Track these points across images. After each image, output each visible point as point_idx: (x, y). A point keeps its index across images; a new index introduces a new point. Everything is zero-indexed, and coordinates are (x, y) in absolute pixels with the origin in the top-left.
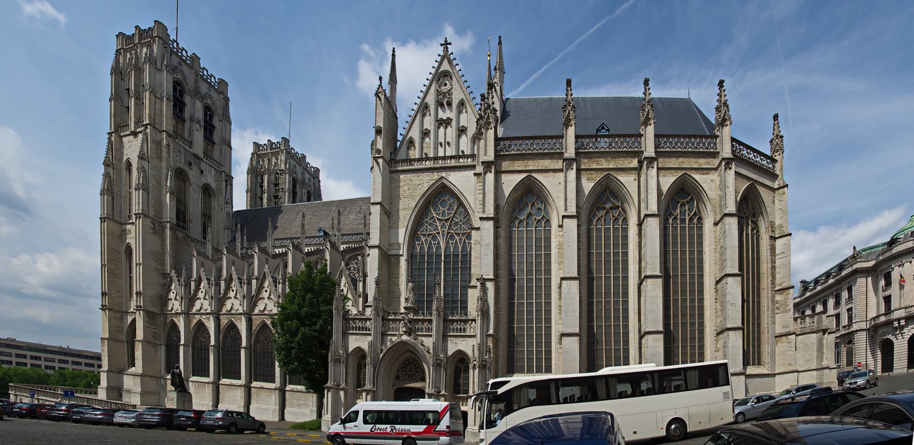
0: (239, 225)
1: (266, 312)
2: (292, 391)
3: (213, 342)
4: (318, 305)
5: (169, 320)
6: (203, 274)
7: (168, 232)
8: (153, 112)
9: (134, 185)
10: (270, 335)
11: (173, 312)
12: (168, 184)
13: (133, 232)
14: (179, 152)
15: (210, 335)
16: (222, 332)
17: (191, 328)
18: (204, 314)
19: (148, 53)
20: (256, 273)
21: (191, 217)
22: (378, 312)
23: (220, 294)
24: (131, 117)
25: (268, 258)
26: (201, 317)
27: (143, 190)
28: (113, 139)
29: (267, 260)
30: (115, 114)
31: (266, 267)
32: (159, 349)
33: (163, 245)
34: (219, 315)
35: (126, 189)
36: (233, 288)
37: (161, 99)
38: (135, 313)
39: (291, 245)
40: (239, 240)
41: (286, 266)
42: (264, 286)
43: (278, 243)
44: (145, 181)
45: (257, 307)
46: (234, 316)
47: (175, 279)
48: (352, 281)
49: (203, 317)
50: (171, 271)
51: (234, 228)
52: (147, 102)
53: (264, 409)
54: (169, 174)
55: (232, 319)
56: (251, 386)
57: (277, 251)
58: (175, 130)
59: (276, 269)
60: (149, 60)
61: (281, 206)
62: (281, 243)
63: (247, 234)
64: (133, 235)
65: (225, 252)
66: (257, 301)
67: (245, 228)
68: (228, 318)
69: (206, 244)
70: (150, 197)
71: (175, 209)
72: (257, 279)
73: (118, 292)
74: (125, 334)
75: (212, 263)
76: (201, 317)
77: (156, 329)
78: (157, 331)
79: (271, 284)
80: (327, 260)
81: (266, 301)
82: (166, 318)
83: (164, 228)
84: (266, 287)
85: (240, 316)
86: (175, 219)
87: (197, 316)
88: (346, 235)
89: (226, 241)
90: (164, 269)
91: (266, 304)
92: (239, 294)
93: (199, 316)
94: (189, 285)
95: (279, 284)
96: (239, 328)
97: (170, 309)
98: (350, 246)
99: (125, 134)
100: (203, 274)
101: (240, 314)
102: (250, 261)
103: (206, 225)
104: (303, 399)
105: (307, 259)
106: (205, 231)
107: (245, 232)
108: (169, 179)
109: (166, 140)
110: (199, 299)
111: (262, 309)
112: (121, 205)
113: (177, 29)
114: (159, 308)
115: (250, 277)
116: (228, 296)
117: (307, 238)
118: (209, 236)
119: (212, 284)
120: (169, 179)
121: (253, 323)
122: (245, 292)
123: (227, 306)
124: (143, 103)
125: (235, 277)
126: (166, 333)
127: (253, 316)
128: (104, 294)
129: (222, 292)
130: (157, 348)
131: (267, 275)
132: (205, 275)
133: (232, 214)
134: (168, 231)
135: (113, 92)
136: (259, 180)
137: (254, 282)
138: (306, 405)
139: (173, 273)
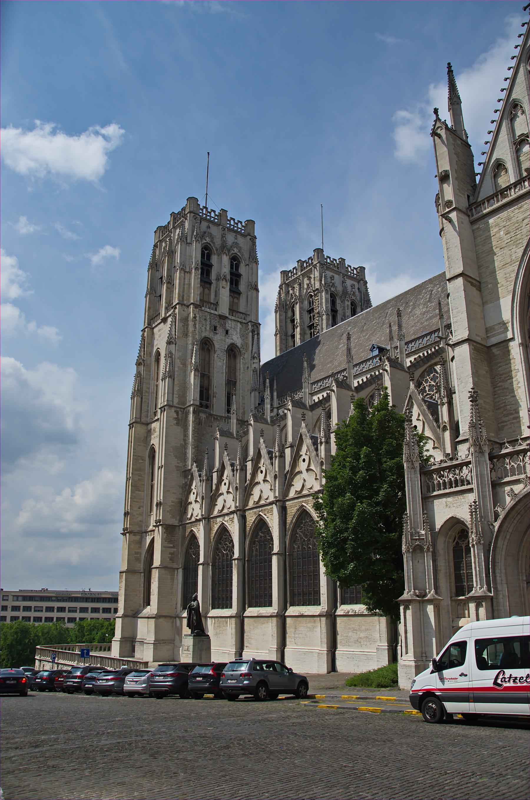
0: (268, 380)
1: (305, 492)
2: (346, 616)
3: (236, 555)
4: (380, 462)
5: (188, 531)
6: (226, 459)
7: (191, 417)
8: (181, 290)
9: (161, 376)
10: (311, 526)
11: (193, 519)
12: (193, 361)
13: (157, 430)
14: (205, 319)
15: (233, 543)
16: (248, 535)
17: (212, 538)
18: (227, 514)
19: (181, 233)
20: (290, 439)
21: (215, 390)
22: (480, 448)
23: (246, 482)
24: (162, 304)
25: (305, 412)
26: (223, 520)
27: (169, 378)
28: (146, 334)
29: (304, 415)
30: (149, 308)
31: (303, 425)
32: (176, 574)
33: (186, 435)
34: (245, 511)
35: (154, 382)
37: (190, 272)
38: (154, 531)
39: (334, 384)
40: (267, 401)
41: (329, 416)
42: (301, 453)
43: (316, 387)
44: (172, 366)
45: (292, 488)
46: (263, 508)
47: (196, 474)
48: (429, 408)
49: (227, 518)
50: (192, 465)
51: (262, 387)
52: (178, 281)
53: (305, 653)
54: (195, 349)
55: (260, 513)
56: (286, 614)
57: (316, 398)
58: (202, 299)
59: (315, 425)
60: (181, 239)
61: (319, 336)
62: (321, 386)
63: (277, 390)
64: (157, 433)
65: (252, 422)
66: (293, 479)
67: (275, 381)
68: (255, 513)
69: (230, 419)
70: (175, 383)
71: (199, 386)
72: (291, 446)
73: (139, 508)
74: (142, 561)
75: (237, 441)
76: (223, 520)
77: (174, 547)
78: (175, 550)
79: (310, 448)
80: (386, 388)
81: (305, 475)
82: (185, 530)
83: (187, 414)
84: (304, 455)
85: (271, 507)
86: (198, 399)
87: (219, 520)
88: (411, 341)
89: (253, 407)
90: (185, 466)
91: (304, 480)
92: (269, 474)
94: (210, 478)
95: (321, 445)
96: (270, 525)
97: (189, 516)
98: (421, 354)
99: (156, 324)
100: (226, 459)
101: (271, 503)
102: (282, 424)
103: (230, 394)
104: (364, 627)
105: (357, 397)
106: (229, 403)
107: (275, 387)
108: (194, 355)
109: (193, 312)
111: (299, 489)
112: (148, 403)
113: (207, 194)
114: (178, 518)
115: (283, 446)
116: (256, 481)
117: (355, 365)
118: (234, 407)
119: (237, 470)
120: (194, 355)
121: (288, 512)
122: (277, 469)
124: (174, 285)
125: (264, 452)
126: (184, 550)
127: (287, 503)
128: (126, 514)
129: (249, 477)
130: (175, 571)
131: (304, 437)
132: (229, 460)
133: (260, 369)
134: (191, 416)
135: (149, 288)
136: (290, 314)
137: (288, 451)
138: (369, 639)
139: (195, 469)
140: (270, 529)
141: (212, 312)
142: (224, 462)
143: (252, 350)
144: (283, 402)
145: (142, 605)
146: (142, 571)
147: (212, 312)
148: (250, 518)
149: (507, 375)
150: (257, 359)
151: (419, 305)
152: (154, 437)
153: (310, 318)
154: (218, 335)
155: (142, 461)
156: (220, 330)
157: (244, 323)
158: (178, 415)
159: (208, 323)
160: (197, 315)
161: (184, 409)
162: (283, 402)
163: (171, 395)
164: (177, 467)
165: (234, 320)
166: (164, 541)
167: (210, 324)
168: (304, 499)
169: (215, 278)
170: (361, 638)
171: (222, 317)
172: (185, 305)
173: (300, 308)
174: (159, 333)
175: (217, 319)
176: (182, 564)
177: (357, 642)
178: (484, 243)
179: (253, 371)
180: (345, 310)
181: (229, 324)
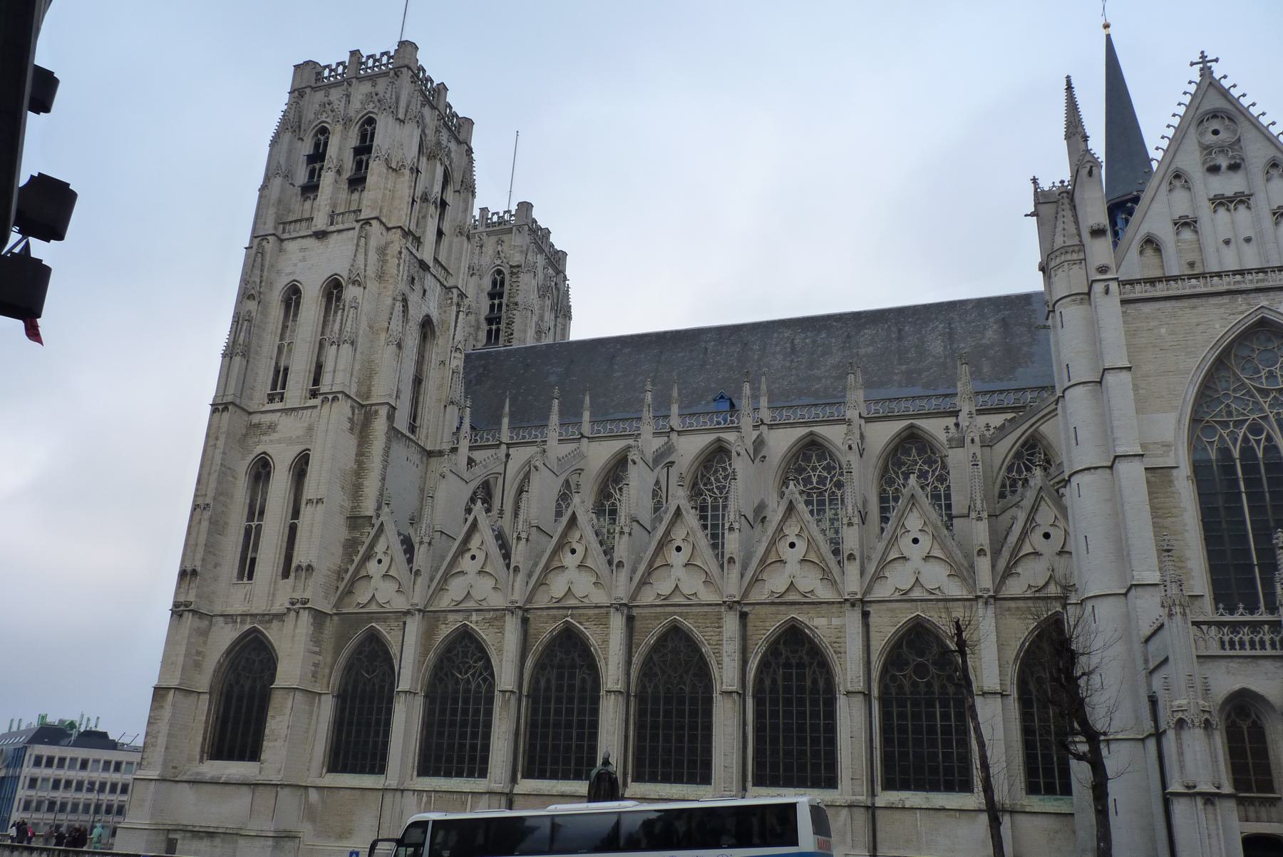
36: (575, 546)
46: (575, 612)
77: (319, 653)
87: (451, 617)
93: (459, 617)
110: (462, 573)
114: (333, 600)
123: (552, 587)
130: (315, 699)
141: (414, 251)
142: (478, 519)
143: (454, 335)
144: (533, 436)
145: (198, 757)
146: (206, 689)
149: (1166, 511)
150: (461, 353)
151: (774, 354)
152: (271, 441)
153: (492, 306)
154: (415, 293)
155: (232, 479)
156: (417, 287)
157: (445, 287)
158: (353, 414)
161: (363, 406)
162: (533, 436)
163: (348, 375)
164: (342, 507)
165: (435, 276)
166: (309, 639)
167: (408, 271)
168: (677, 610)
169: (420, 196)
171: (423, 266)
172: (384, 225)
173: (479, 286)
174: (302, 254)
175: (417, 265)
176: (333, 688)
178: (1134, 335)
179: (453, 372)
180: (543, 310)
181: (429, 282)
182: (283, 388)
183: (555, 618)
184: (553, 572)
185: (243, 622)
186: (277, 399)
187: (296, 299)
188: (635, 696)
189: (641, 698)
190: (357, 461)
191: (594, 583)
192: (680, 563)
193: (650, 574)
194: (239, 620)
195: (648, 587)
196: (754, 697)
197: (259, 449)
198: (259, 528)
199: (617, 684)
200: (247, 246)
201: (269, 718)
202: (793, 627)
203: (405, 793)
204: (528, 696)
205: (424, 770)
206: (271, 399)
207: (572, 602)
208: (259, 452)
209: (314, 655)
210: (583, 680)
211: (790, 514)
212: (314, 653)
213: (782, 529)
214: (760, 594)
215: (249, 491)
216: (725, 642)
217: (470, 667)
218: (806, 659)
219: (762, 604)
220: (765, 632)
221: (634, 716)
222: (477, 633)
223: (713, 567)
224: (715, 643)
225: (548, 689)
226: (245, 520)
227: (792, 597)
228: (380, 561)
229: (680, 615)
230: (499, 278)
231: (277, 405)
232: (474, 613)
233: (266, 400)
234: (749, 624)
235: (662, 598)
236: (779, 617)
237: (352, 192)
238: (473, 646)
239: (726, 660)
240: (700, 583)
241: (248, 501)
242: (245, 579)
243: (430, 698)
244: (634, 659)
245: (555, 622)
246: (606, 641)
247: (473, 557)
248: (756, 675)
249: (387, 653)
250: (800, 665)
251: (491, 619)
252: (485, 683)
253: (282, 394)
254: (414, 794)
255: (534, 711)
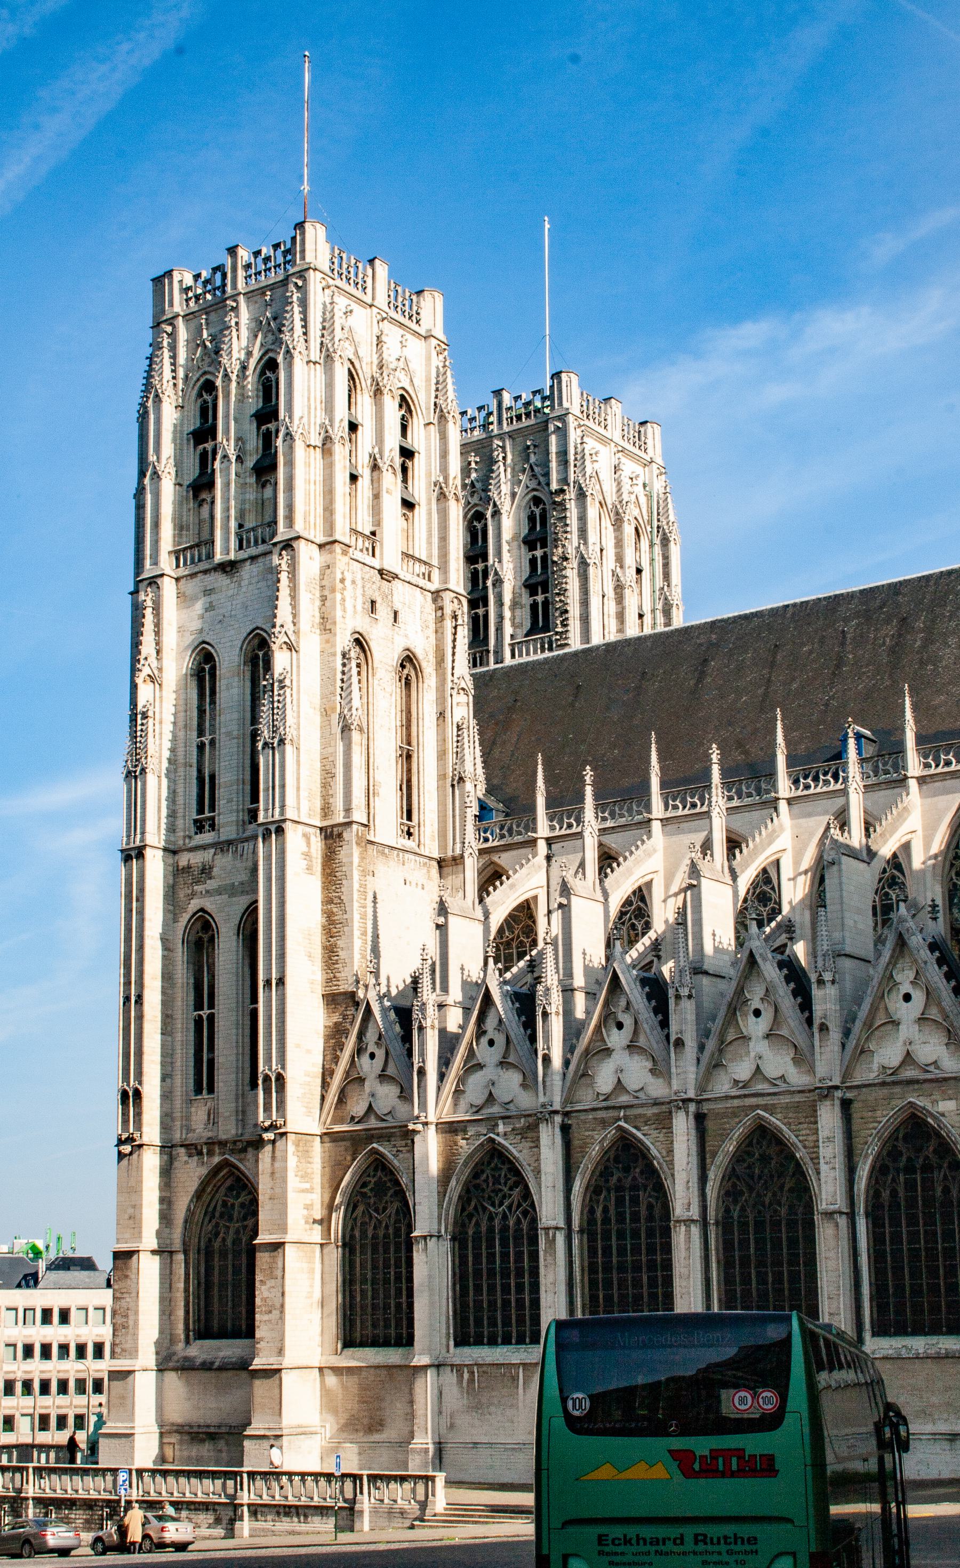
46: (630, 1112)
104: (940, 1384)
140: (655, 1162)
141: (368, 560)
145: (182, 1337)
147: (368, 560)
148: (587, 1133)
152: (207, 892)
153: (533, 561)
154: (380, 624)
156: (383, 612)
159: (359, 591)
160: (346, 573)
167: (363, 595)
170: (933, 1406)
177: (923, 1415)
182: (212, 808)
183: (604, 1123)
184: (595, 1058)
185: (211, 1153)
186: (207, 827)
187: (210, 669)
188: (717, 1223)
189: (725, 1224)
190: (324, 912)
191: (651, 1070)
192: (760, 1034)
193: (721, 1051)
194: (205, 1151)
195: (722, 1073)
196: (867, 1215)
197: (194, 905)
198: (211, 1018)
199: (688, 1210)
200: (132, 589)
201: (257, 1284)
202: (913, 1116)
203: (441, 1369)
204: (581, 1231)
205: (462, 1340)
206: (199, 826)
207: (624, 1099)
208: (195, 910)
209: (302, 1195)
210: (650, 1207)
211: (902, 952)
212: (303, 1191)
213: (891, 976)
214: (868, 1073)
215: (191, 966)
216: (821, 1145)
217: (504, 1197)
218: (934, 1160)
219: (870, 1085)
220: (876, 1125)
221: (717, 1249)
222: (507, 1150)
223: (801, 1040)
224: (812, 1144)
225: (606, 1220)
226: (192, 1008)
227: (910, 1073)
228: (372, 1056)
229: (765, 1108)
230: (537, 511)
231: (207, 837)
232: (500, 1122)
233: (193, 829)
234: (854, 1115)
235: (741, 1085)
236: (894, 1102)
237: (263, 486)
238: (505, 1168)
239: (823, 1168)
240: (788, 1059)
241: (192, 981)
242: (205, 1092)
243: (459, 1239)
244: (711, 1175)
245: (604, 1128)
246: (670, 1151)
247: (491, 1043)
248: (868, 1185)
249: (397, 1183)
250: (927, 1168)
251: (522, 1128)
252: (525, 1218)
253: (213, 819)
254: (452, 1371)
255: (592, 1251)
